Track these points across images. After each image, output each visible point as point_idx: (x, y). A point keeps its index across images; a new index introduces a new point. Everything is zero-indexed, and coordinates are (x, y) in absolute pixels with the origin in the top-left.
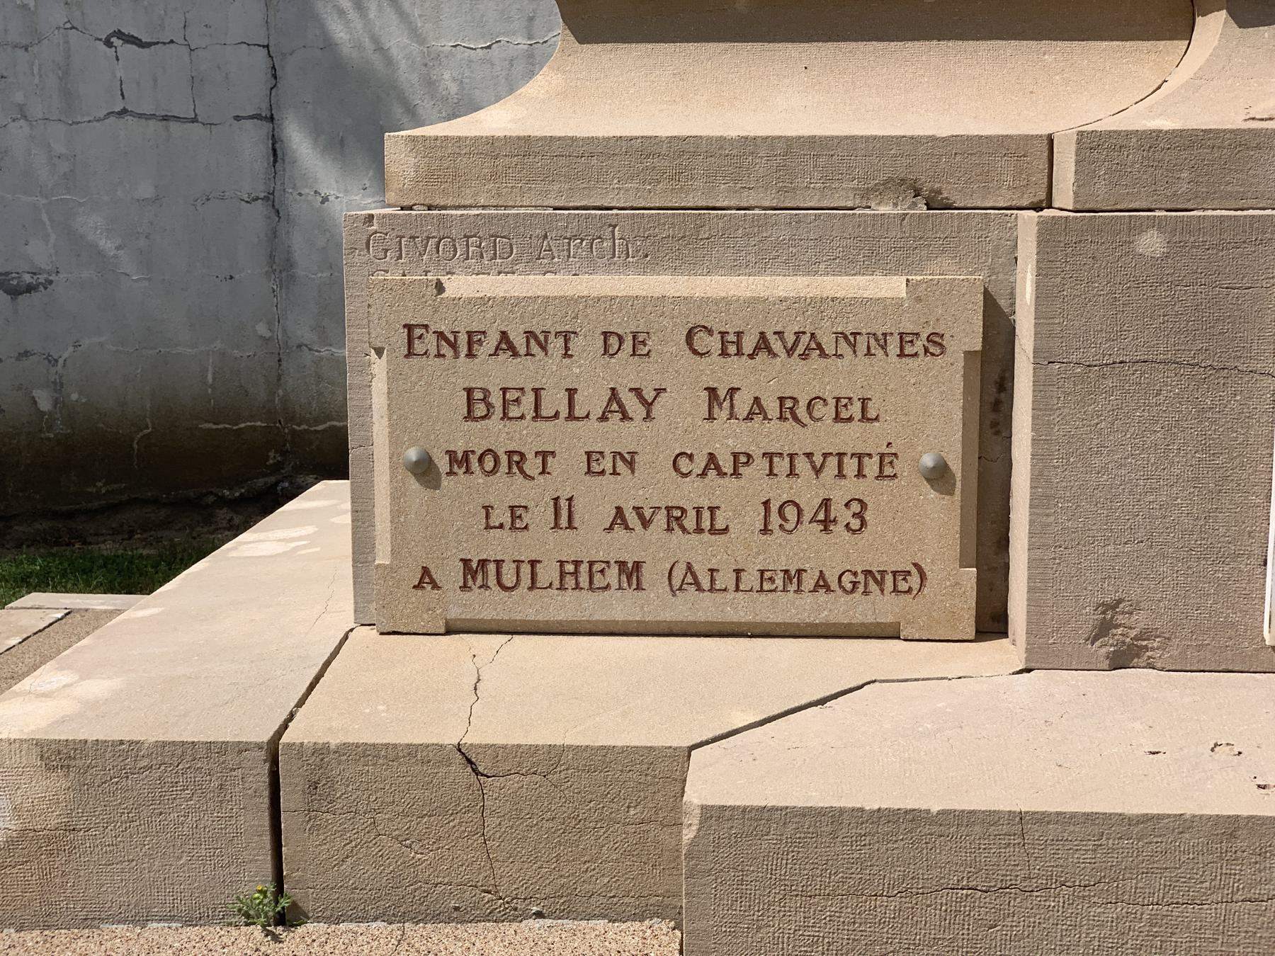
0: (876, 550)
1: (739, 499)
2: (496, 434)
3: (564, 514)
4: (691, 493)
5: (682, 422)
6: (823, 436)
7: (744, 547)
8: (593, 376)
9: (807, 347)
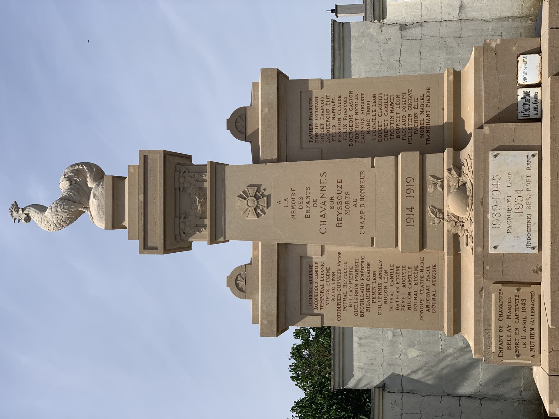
1: (522, 315)
2: (513, 346)
3: (524, 338)
4: (521, 321)
5: (512, 322)
6: (513, 304)
7: (528, 314)
8: (505, 333)
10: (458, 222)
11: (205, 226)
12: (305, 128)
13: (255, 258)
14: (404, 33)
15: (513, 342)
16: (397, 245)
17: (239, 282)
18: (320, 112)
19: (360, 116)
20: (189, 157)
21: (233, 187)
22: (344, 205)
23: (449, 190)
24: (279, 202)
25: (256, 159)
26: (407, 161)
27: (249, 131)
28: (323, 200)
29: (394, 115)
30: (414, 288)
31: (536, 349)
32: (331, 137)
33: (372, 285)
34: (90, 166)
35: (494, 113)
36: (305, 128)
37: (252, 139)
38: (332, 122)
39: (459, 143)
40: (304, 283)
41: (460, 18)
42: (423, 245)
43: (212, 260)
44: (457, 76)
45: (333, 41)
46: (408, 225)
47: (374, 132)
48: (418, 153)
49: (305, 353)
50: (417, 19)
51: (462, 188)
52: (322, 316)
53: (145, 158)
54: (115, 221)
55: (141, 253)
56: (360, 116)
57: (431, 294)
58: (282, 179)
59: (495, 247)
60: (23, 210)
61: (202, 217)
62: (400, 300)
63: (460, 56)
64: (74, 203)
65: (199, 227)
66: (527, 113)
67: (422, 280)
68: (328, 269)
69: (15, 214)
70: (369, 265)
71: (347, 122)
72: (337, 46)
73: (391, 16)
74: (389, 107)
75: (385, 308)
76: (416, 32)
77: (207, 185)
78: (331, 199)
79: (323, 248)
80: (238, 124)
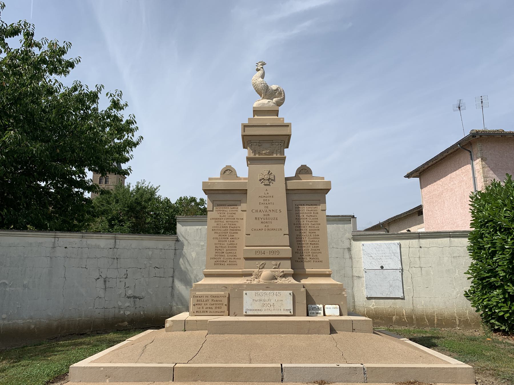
0: (222, 310)
1: (214, 307)
2: (199, 303)
3: (203, 308)
4: (211, 306)
5: (210, 302)
6: (219, 302)
7: (214, 310)
8: (205, 299)
9: (218, 297)
10: (258, 276)
11: (255, 155)
12: (302, 202)
13: (240, 179)
14: (346, 250)
15: (200, 303)
16: (247, 246)
17: (228, 171)
18: (310, 209)
19: (308, 229)
20: (288, 147)
21: (273, 168)
22: (265, 221)
23: (273, 271)
24: (267, 190)
25: (287, 179)
26: (287, 252)
27: (300, 176)
28: (268, 211)
29: (309, 245)
30: (226, 255)
31: (198, 314)
32: (298, 214)
33: (227, 234)
34: (284, 99)
35: (311, 293)
36: (302, 202)
37: (297, 177)
38: (305, 215)
39: (295, 276)
40: (228, 202)
42: (246, 259)
43: (238, 158)
44: (328, 275)
45: (342, 216)
46: (257, 252)
47: (301, 235)
48: (290, 256)
49: (193, 204)
50: (353, 256)
51: (274, 278)
52: (212, 211)
53: (287, 126)
54: (256, 112)
55: (242, 124)
56: (308, 229)
57: (223, 263)
58: (278, 191)
59: (246, 294)
60: (262, 68)
61: (259, 154)
62: (220, 248)
64: (265, 92)
65: (254, 152)
67: (230, 259)
68: (235, 214)
69: (260, 64)
70: (237, 233)
71: (305, 222)
72: (340, 218)
73: (354, 243)
74: (313, 243)
75: (216, 241)
76: (347, 256)
77: (275, 156)
78: (269, 215)
79: (245, 211)
80: (304, 170)
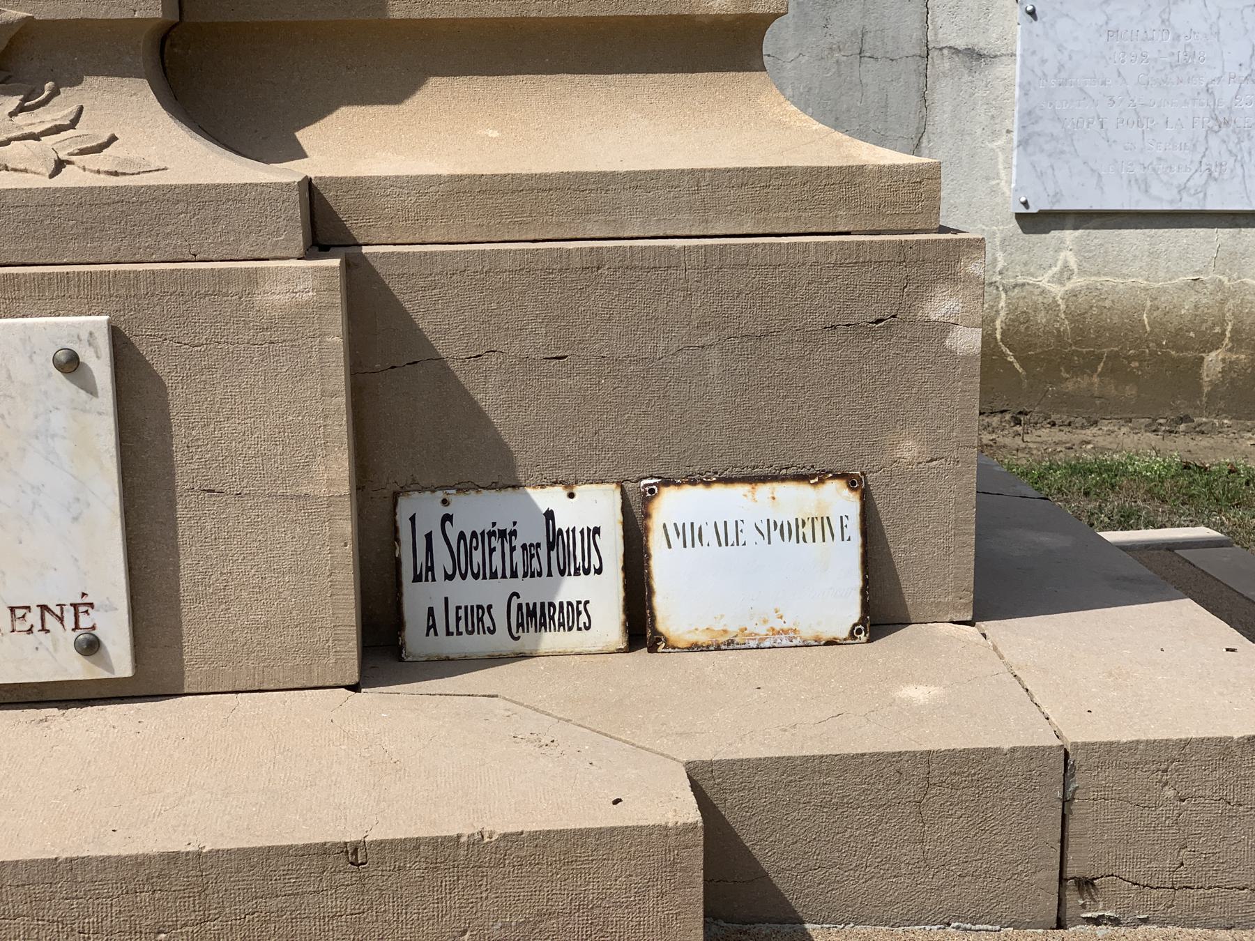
35: (442, 323)
41: (933, 54)
63: (791, 55)
66: (442, 560)
